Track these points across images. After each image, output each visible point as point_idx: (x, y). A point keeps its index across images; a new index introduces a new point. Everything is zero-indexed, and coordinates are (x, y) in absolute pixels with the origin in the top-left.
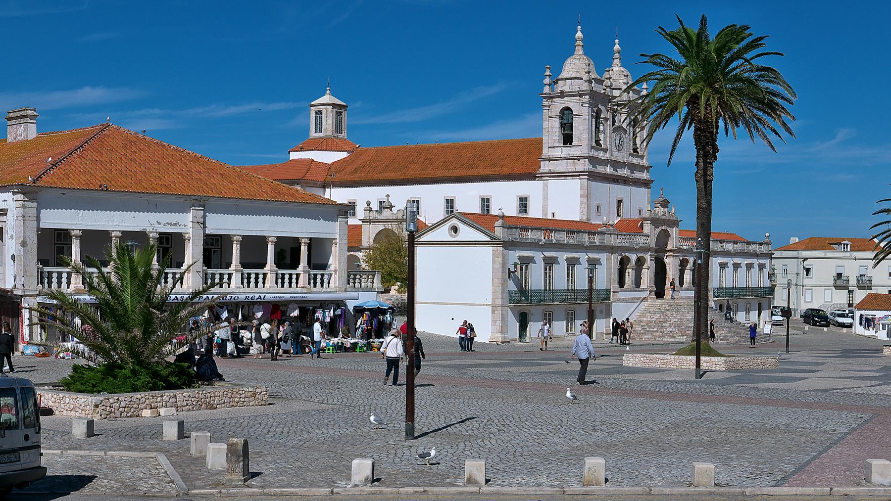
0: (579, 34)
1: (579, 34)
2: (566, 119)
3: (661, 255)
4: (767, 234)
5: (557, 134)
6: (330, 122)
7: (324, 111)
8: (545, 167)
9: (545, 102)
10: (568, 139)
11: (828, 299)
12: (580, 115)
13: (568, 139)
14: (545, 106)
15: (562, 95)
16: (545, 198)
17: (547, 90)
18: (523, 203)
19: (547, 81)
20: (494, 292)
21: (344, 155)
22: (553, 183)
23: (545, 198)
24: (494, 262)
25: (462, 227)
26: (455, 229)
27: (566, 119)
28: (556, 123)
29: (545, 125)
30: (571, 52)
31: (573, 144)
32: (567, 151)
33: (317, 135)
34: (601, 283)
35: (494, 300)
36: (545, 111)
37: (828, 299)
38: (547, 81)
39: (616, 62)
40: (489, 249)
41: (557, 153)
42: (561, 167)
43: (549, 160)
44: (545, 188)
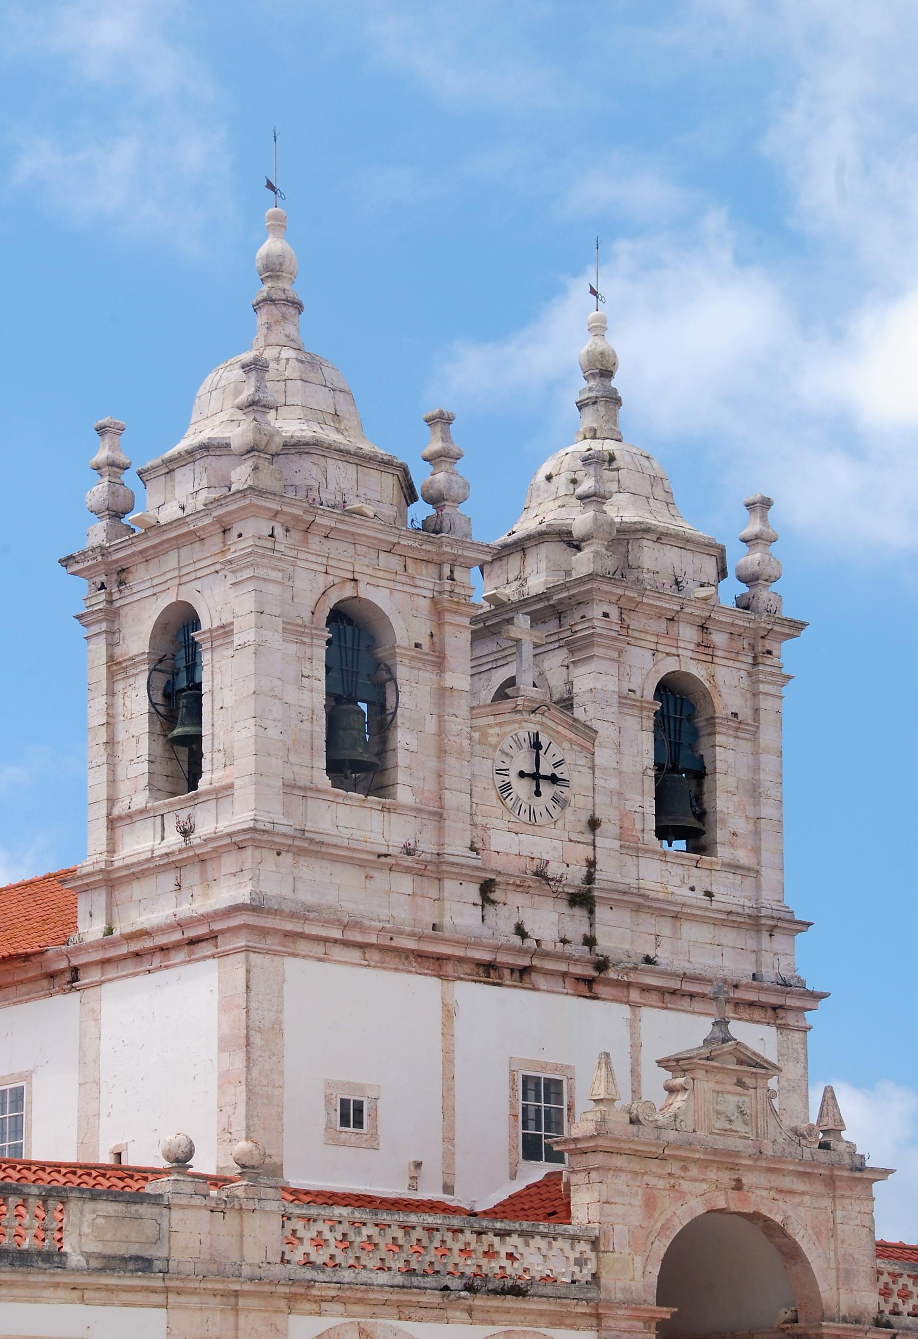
5: (144, 748)
12: (226, 630)
42: (154, 909)
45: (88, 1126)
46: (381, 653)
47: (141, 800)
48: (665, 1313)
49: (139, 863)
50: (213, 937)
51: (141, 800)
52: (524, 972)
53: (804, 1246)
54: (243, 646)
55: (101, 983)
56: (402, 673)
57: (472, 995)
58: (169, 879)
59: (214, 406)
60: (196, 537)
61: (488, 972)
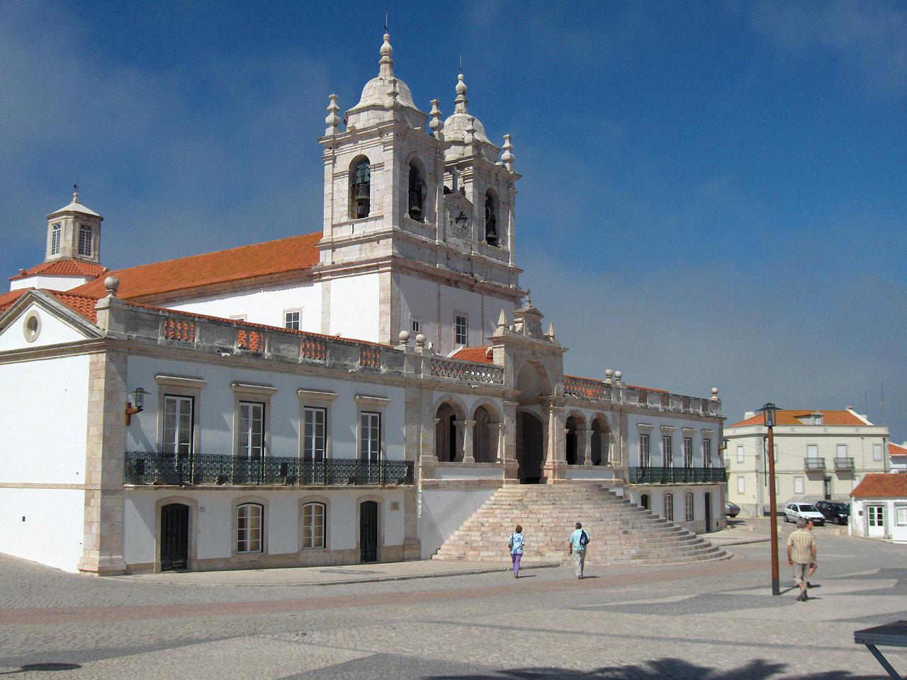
0: (386, 46)
1: (386, 46)
2: (359, 174)
3: (536, 409)
4: (714, 390)
6: (70, 237)
7: (63, 222)
8: (326, 258)
9: (328, 152)
10: (360, 206)
11: (799, 490)
12: (381, 165)
13: (360, 206)
14: (328, 158)
15: (356, 136)
16: (326, 312)
17: (330, 131)
18: (293, 318)
19: (330, 118)
20: (90, 460)
21: (80, 282)
22: (341, 286)
23: (326, 312)
24: (91, 389)
25: (45, 317)
26: (33, 324)
27: (359, 174)
28: (344, 185)
29: (327, 189)
30: (374, 73)
31: (370, 215)
32: (363, 228)
33: (57, 256)
34: (394, 451)
35: (89, 473)
36: (328, 169)
37: (799, 490)
38: (330, 118)
39: (459, 106)
40: (82, 364)
41: (344, 233)
43: (333, 246)
44: (328, 290)
45: (326, 324)
46: (421, 176)
47: (345, 219)
48: (519, 392)
49: (346, 240)
50: (377, 267)
51: (345, 219)
52: (457, 282)
53: (548, 372)
54: (388, 171)
55: (331, 279)
56: (427, 182)
57: (445, 289)
58: (358, 246)
59: (371, 93)
60: (371, 136)
61: (448, 282)
